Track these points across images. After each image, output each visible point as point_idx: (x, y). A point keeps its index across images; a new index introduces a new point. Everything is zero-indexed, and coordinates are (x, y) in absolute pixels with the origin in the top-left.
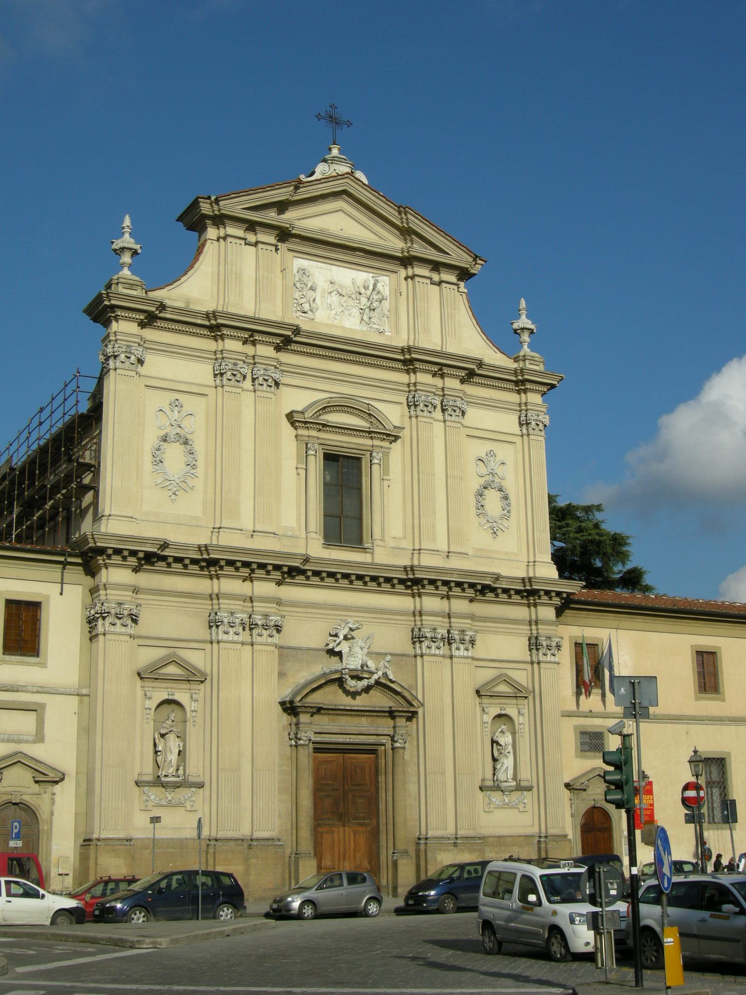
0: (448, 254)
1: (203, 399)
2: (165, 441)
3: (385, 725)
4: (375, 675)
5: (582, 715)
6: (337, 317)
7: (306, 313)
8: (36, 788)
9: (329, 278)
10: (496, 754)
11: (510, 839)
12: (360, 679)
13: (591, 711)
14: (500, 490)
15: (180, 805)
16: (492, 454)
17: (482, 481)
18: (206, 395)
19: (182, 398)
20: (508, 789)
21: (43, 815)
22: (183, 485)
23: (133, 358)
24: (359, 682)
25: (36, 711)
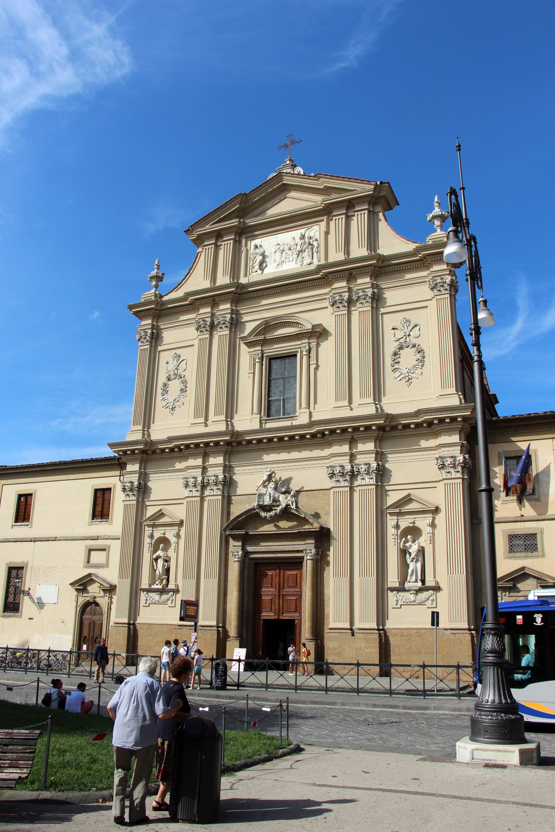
0: (355, 190)
1: (192, 348)
2: (169, 380)
3: (298, 545)
4: (280, 507)
5: (510, 520)
6: (279, 266)
7: (257, 271)
8: (102, 593)
9: (275, 244)
10: (409, 561)
11: (415, 631)
12: (270, 510)
13: (522, 516)
14: (414, 346)
15: (165, 603)
16: (405, 321)
17: (397, 343)
18: (193, 345)
19: (177, 351)
20: (412, 588)
21: (105, 610)
22: (177, 404)
23: (148, 337)
24: (268, 513)
25: (104, 550)
